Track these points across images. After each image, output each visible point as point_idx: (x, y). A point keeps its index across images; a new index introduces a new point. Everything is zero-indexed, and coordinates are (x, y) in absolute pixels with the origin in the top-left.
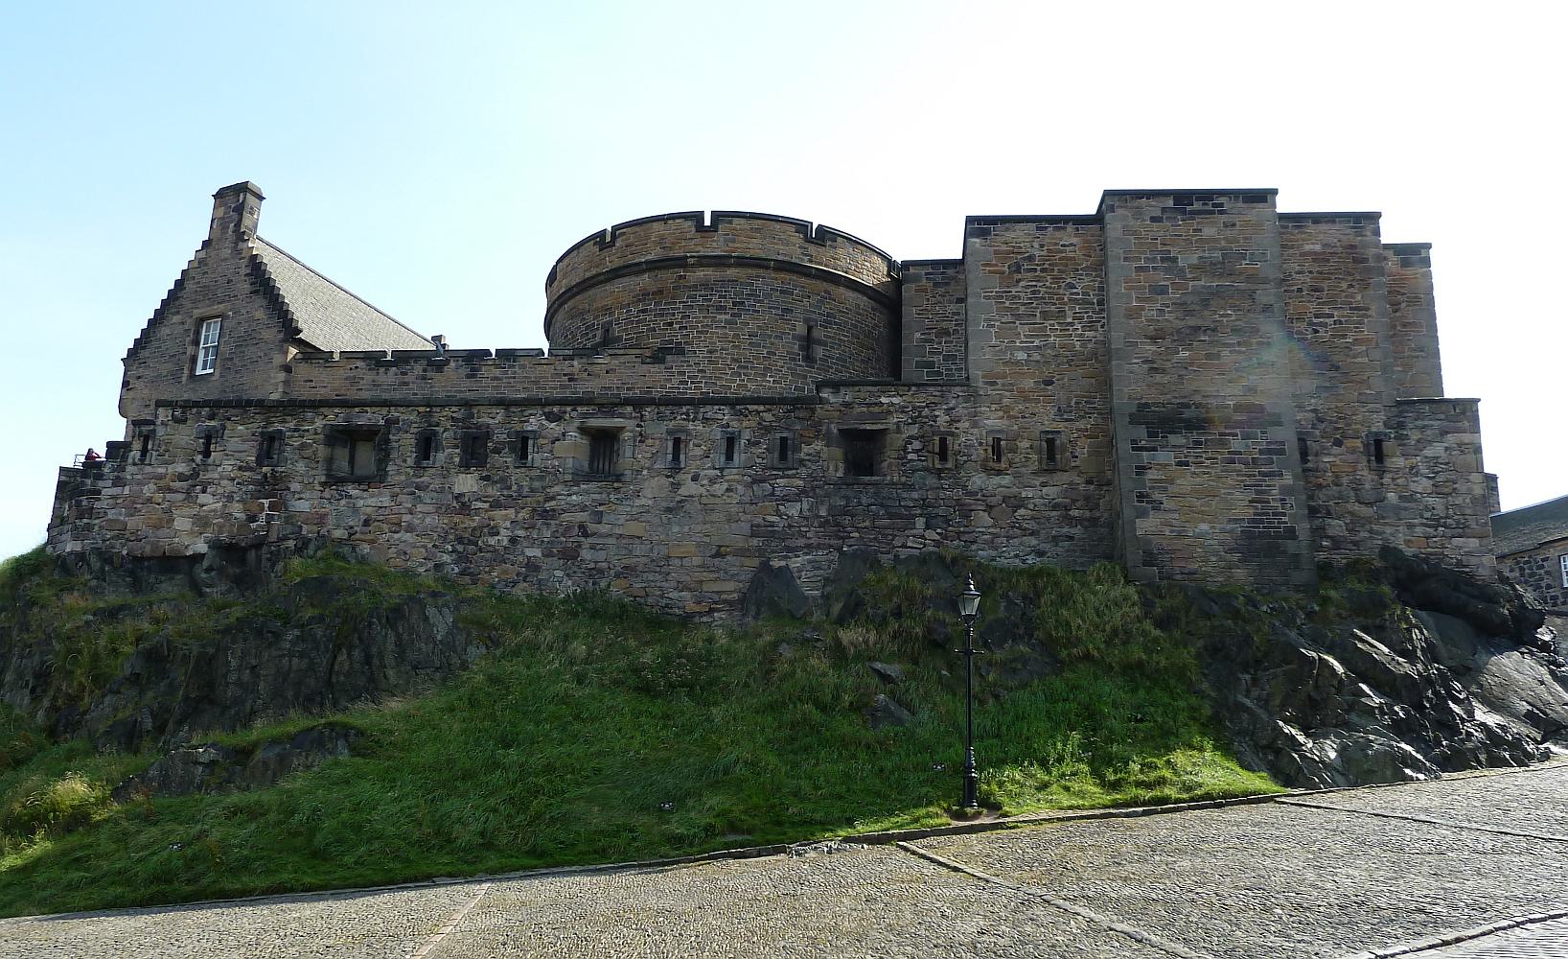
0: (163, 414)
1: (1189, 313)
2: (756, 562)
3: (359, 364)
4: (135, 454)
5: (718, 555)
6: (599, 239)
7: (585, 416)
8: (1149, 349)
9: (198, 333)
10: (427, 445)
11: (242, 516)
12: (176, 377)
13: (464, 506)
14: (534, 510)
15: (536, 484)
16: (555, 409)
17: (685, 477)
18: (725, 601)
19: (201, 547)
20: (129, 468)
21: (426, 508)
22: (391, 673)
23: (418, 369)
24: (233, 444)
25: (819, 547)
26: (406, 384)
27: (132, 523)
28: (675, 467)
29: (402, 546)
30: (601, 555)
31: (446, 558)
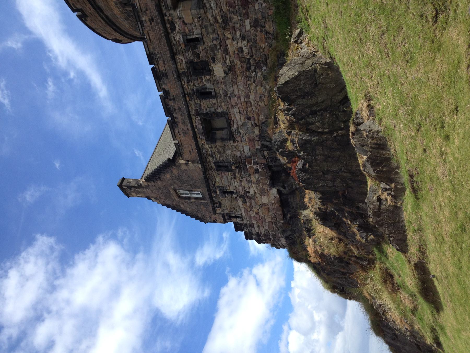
0: (219, 211)
3: (176, 131)
4: (238, 220)
6: (83, 18)
7: (167, 7)
9: (185, 198)
10: (204, 94)
11: (257, 176)
12: (205, 205)
13: (230, 70)
14: (224, 29)
15: (210, 30)
16: (168, 26)
19: (274, 191)
20: (245, 222)
21: (236, 90)
22: (320, 99)
23: (171, 103)
24: (225, 182)
26: (179, 108)
27: (268, 219)
29: (257, 99)
31: (259, 75)
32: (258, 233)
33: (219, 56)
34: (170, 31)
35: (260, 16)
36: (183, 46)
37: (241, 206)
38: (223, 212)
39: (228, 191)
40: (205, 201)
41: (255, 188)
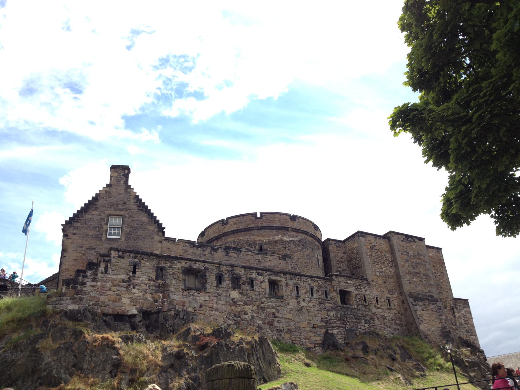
0: (113, 253)
1: (414, 268)
2: (324, 331)
4: (102, 269)
5: (313, 327)
8: (408, 277)
9: (108, 220)
13: (235, 303)
15: (258, 297)
16: (260, 272)
17: (301, 299)
18: (318, 344)
19: (135, 312)
20: (99, 275)
24: (145, 270)
25: (339, 327)
26: (205, 255)
27: (103, 299)
28: (298, 297)
29: (215, 316)
30: (281, 325)
31: (231, 322)
32: (85, 284)
33: (243, 298)
34: (258, 271)
35: (264, 331)
36: (249, 276)
37: (119, 276)
38: (112, 256)
39: (137, 270)
40: (103, 239)
41: (139, 294)
